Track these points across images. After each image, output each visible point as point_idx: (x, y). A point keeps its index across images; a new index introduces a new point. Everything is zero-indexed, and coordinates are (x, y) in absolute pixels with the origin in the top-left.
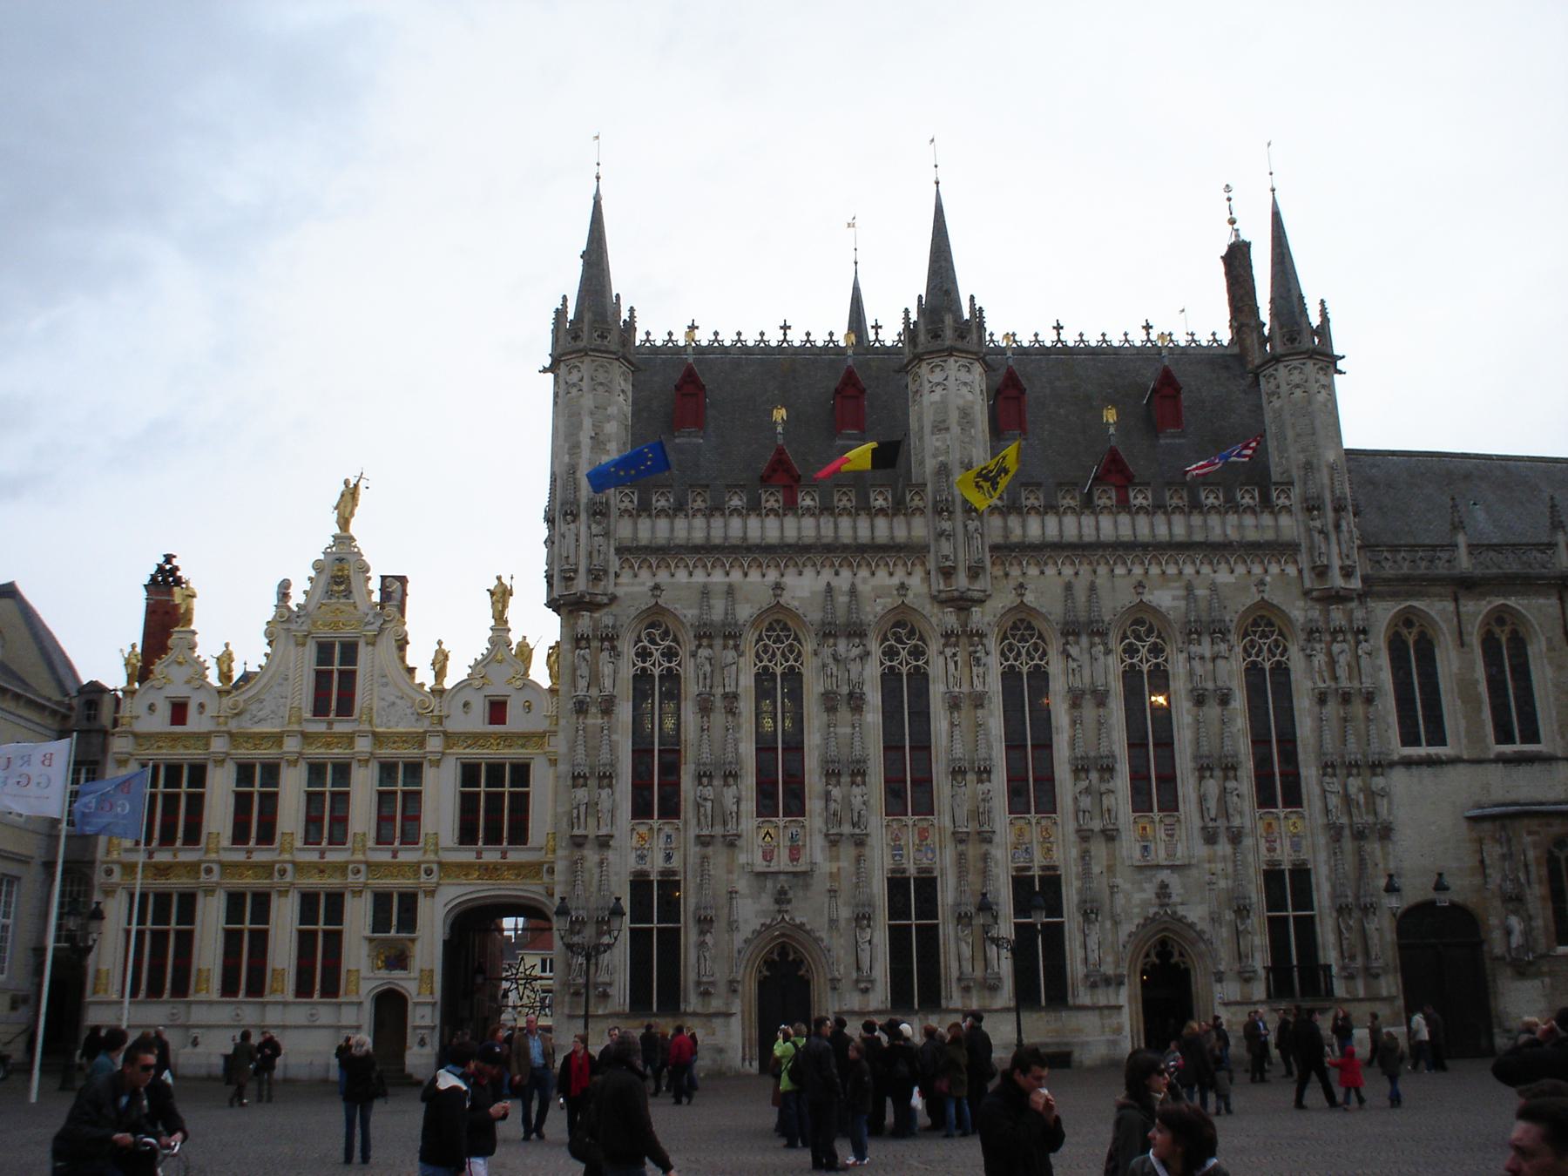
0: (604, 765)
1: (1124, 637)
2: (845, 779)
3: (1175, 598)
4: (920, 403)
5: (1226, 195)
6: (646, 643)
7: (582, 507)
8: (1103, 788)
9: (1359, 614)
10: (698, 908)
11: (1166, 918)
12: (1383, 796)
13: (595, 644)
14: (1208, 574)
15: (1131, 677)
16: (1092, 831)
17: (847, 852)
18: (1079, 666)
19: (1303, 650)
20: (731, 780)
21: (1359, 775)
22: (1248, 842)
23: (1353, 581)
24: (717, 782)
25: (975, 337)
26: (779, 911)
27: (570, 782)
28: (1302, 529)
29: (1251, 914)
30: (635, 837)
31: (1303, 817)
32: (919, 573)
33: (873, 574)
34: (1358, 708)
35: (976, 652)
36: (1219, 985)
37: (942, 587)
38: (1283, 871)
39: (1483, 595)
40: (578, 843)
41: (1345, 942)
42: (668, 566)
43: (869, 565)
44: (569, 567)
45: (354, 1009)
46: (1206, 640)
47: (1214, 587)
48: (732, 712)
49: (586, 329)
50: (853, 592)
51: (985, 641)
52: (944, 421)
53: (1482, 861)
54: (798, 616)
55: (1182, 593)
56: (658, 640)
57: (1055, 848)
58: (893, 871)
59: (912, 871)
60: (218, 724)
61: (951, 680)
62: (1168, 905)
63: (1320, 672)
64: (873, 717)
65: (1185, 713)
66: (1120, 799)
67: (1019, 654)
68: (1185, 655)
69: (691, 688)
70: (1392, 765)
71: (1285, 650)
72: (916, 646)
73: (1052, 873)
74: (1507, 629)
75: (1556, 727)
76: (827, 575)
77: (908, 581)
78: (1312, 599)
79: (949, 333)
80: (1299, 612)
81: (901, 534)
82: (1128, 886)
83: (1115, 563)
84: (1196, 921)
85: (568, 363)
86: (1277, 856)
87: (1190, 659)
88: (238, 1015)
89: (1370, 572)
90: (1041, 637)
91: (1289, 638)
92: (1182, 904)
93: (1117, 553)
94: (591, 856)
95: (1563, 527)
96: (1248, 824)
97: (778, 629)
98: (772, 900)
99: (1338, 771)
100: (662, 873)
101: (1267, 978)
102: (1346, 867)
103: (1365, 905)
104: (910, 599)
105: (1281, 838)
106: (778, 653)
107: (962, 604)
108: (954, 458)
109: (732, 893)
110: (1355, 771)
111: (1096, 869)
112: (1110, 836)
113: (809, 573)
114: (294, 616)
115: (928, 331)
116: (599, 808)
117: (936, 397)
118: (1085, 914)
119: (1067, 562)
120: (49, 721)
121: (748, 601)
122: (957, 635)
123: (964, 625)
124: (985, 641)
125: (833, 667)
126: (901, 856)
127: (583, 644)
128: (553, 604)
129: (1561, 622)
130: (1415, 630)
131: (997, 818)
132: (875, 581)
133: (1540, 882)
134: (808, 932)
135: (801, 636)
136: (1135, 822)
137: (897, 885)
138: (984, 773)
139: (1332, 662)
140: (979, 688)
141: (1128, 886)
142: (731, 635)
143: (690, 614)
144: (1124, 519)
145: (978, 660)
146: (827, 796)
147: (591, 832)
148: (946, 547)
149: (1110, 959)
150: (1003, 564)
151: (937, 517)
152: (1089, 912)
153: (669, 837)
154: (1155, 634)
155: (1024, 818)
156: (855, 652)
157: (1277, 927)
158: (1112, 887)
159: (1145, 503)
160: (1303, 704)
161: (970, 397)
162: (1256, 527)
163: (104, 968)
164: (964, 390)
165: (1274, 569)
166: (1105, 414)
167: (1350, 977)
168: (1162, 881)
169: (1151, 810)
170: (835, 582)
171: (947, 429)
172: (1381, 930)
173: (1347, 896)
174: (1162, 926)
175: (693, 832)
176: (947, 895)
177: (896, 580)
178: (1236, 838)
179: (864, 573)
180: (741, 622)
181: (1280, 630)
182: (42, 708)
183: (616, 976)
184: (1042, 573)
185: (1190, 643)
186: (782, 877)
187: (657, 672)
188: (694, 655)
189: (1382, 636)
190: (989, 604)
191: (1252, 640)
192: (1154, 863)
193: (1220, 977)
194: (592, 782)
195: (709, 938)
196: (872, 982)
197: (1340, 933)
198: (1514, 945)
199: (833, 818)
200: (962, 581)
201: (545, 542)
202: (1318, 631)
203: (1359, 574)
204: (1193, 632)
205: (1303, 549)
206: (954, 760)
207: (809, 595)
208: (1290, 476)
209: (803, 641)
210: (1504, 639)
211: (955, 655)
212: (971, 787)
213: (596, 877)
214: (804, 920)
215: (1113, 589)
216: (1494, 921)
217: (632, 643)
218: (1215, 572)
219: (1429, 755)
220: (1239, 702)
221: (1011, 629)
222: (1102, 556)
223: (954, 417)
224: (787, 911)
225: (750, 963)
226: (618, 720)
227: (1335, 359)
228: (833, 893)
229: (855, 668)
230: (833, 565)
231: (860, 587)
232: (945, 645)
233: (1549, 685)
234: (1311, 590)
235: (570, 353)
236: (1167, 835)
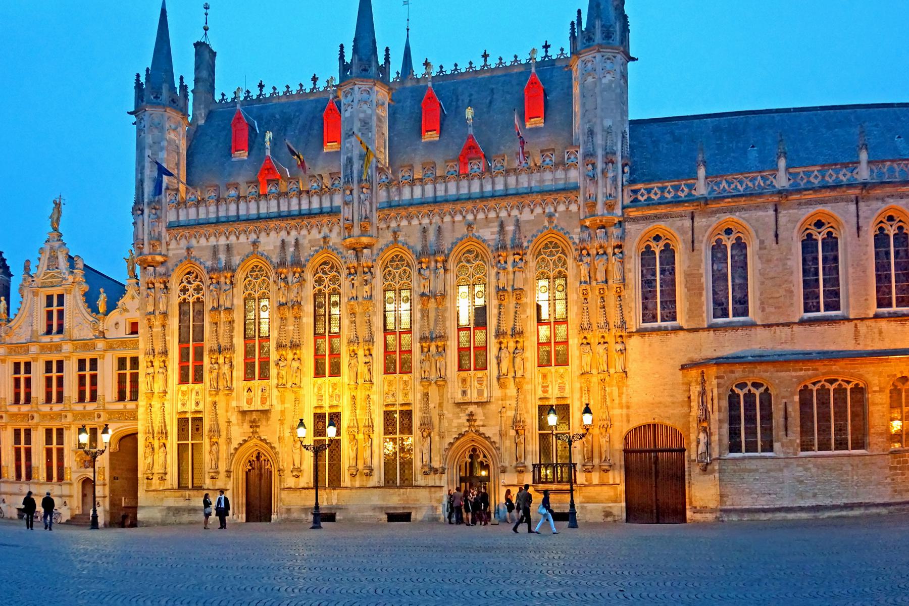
3: (492, 233)
14: (516, 216)
22: (527, 387)
50: (297, 244)
53: (689, 398)
55: (497, 229)
58: (316, 407)
62: (474, 426)
66: (448, 364)
82: (450, 415)
84: (490, 436)
86: (546, 395)
92: (483, 426)
111: (432, 406)
126: (321, 400)
133: (720, 411)
141: (450, 415)
144: (464, 183)
153: (197, 393)
165: (561, 208)
168: (471, 412)
181: (563, 249)
192: (469, 401)
193: (504, 471)
198: (699, 452)
216: (693, 437)
218: (521, 214)
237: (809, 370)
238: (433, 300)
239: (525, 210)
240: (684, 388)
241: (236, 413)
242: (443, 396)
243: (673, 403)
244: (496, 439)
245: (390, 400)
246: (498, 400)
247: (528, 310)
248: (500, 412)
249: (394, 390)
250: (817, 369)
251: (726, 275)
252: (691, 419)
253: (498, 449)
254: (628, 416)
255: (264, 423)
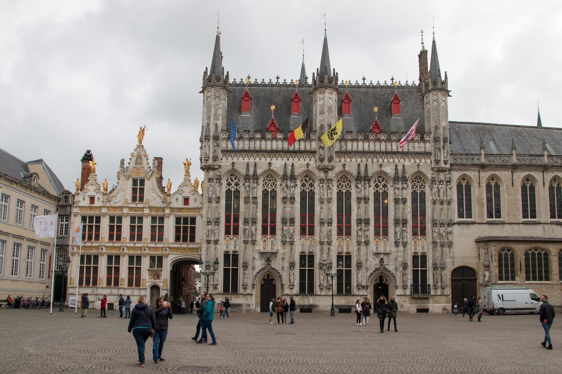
0: (216, 219)
1: (375, 182)
2: (288, 224)
3: (391, 169)
4: (316, 104)
5: (421, 34)
6: (230, 181)
7: (211, 137)
8: (366, 228)
9: (448, 176)
10: (243, 263)
11: (382, 269)
12: (450, 234)
13: (215, 181)
15: (376, 194)
16: (361, 242)
17: (288, 246)
18: (361, 191)
19: (430, 186)
20: (254, 224)
21: (444, 227)
22: (408, 246)
23: (447, 165)
24: (250, 224)
25: (334, 83)
26: (267, 264)
27: (206, 224)
28: (433, 148)
29: (408, 269)
30: (225, 240)
31: (426, 240)
32: (313, 160)
33: (299, 160)
34: (445, 206)
35: (329, 185)
36: (396, 290)
37: (320, 164)
38: (418, 256)
39: (488, 170)
40: (209, 242)
41: (435, 278)
42: (237, 157)
43: (298, 157)
44: (206, 156)
45: (145, 290)
46: (400, 183)
47: (404, 166)
48: (255, 203)
49: (213, 79)
51: (332, 182)
52: (323, 111)
53: (479, 255)
54: (276, 173)
55: (394, 168)
56: (233, 180)
57: (350, 247)
58: (301, 253)
59: (307, 253)
60: (104, 204)
61: (321, 194)
63: (435, 194)
64: (297, 205)
65: (392, 206)
66: (370, 233)
67: (343, 186)
68: (393, 188)
69: (243, 195)
70: (454, 224)
71: (424, 186)
72: (311, 183)
73: (348, 255)
74: (494, 181)
75: (506, 213)
76: (285, 160)
77: (310, 163)
78: (434, 171)
79: (326, 81)
80: (429, 174)
81: (308, 148)
83: (374, 158)
85: (207, 90)
86: (416, 251)
87: (395, 189)
88: (111, 292)
89: (453, 162)
90: (349, 181)
91: (426, 183)
92: (387, 265)
93: (375, 155)
94: (212, 246)
95: (515, 149)
96: (409, 241)
97: (270, 177)
98: (265, 261)
99: (437, 225)
100: (233, 252)
101: (411, 288)
102: (437, 255)
103: (442, 267)
104: (310, 168)
105: (419, 245)
106: (270, 185)
107: (326, 170)
108: (326, 123)
109: (254, 258)
110: (442, 226)
111: (362, 254)
112: (367, 243)
113: (280, 159)
114: (125, 170)
115: (319, 81)
116: (215, 232)
117: (321, 103)
118: (358, 267)
119: (359, 157)
120: (54, 202)
121: (261, 168)
122: (324, 180)
123: (326, 177)
124: (332, 182)
125: (286, 189)
127: (211, 181)
128: (202, 168)
129: (511, 179)
130: (465, 181)
131: (333, 238)
132: (300, 162)
134: (276, 270)
135: (277, 179)
136: (375, 240)
137: (302, 257)
138: (330, 223)
139: (439, 191)
140: (330, 196)
141: (371, 259)
142: (255, 177)
143: (244, 172)
144: (378, 144)
145: (330, 188)
146: (283, 229)
147: (213, 239)
148: (322, 152)
149: (365, 281)
150: (339, 157)
151: (319, 142)
152: (359, 265)
153: (235, 241)
154: (385, 181)
155: (341, 238)
156: (293, 184)
157: (415, 272)
158: (366, 259)
159: (384, 138)
160: (428, 204)
161: (332, 103)
162: (419, 147)
163: (72, 277)
164: (330, 100)
165: (423, 161)
166: (374, 109)
167: (436, 289)
168: (382, 258)
169: (380, 236)
170: (287, 163)
171: (324, 113)
172: (447, 275)
173: (437, 264)
174: (381, 271)
175: (242, 240)
176: (317, 261)
177: (306, 162)
178: (405, 245)
179: (296, 159)
180: (258, 175)
182: (52, 198)
183: (219, 282)
184: (351, 161)
185: (395, 184)
186: (268, 254)
187: (233, 190)
188: (244, 184)
189: (455, 183)
190: (333, 170)
191: (414, 184)
194: (213, 224)
195: (246, 272)
196: (293, 285)
197: (434, 275)
199: (284, 236)
200: (326, 163)
201: (200, 148)
202: (435, 181)
203: (449, 163)
204: (396, 179)
205: (433, 154)
206: (321, 219)
207: (279, 166)
208: (430, 131)
209: (277, 181)
210: (493, 185)
211: (323, 186)
212: (326, 228)
213: (214, 253)
214: (274, 267)
215: (373, 165)
216: (481, 273)
217: (226, 181)
218: (405, 161)
219: (466, 221)
220: (409, 203)
221: (341, 178)
222: (370, 155)
223: (326, 109)
224: (270, 264)
225: (258, 280)
226: (221, 205)
227: (448, 92)
228: (283, 259)
229: (292, 190)
230: (287, 157)
231: (295, 164)
232: (320, 183)
233: (506, 200)
234: (434, 168)
235: (207, 87)
236: (384, 244)
237: (528, 244)
238: (363, 200)
239: (406, 159)
240: (476, 250)
241: (258, 253)
242: (367, 249)
243: (472, 257)
244: (393, 271)
245: (340, 250)
246: (394, 252)
247: (408, 209)
248: (396, 259)
249: (342, 244)
250: (531, 245)
251: (492, 199)
252: (480, 265)
253: (394, 277)
254: (453, 262)
255: (274, 259)
